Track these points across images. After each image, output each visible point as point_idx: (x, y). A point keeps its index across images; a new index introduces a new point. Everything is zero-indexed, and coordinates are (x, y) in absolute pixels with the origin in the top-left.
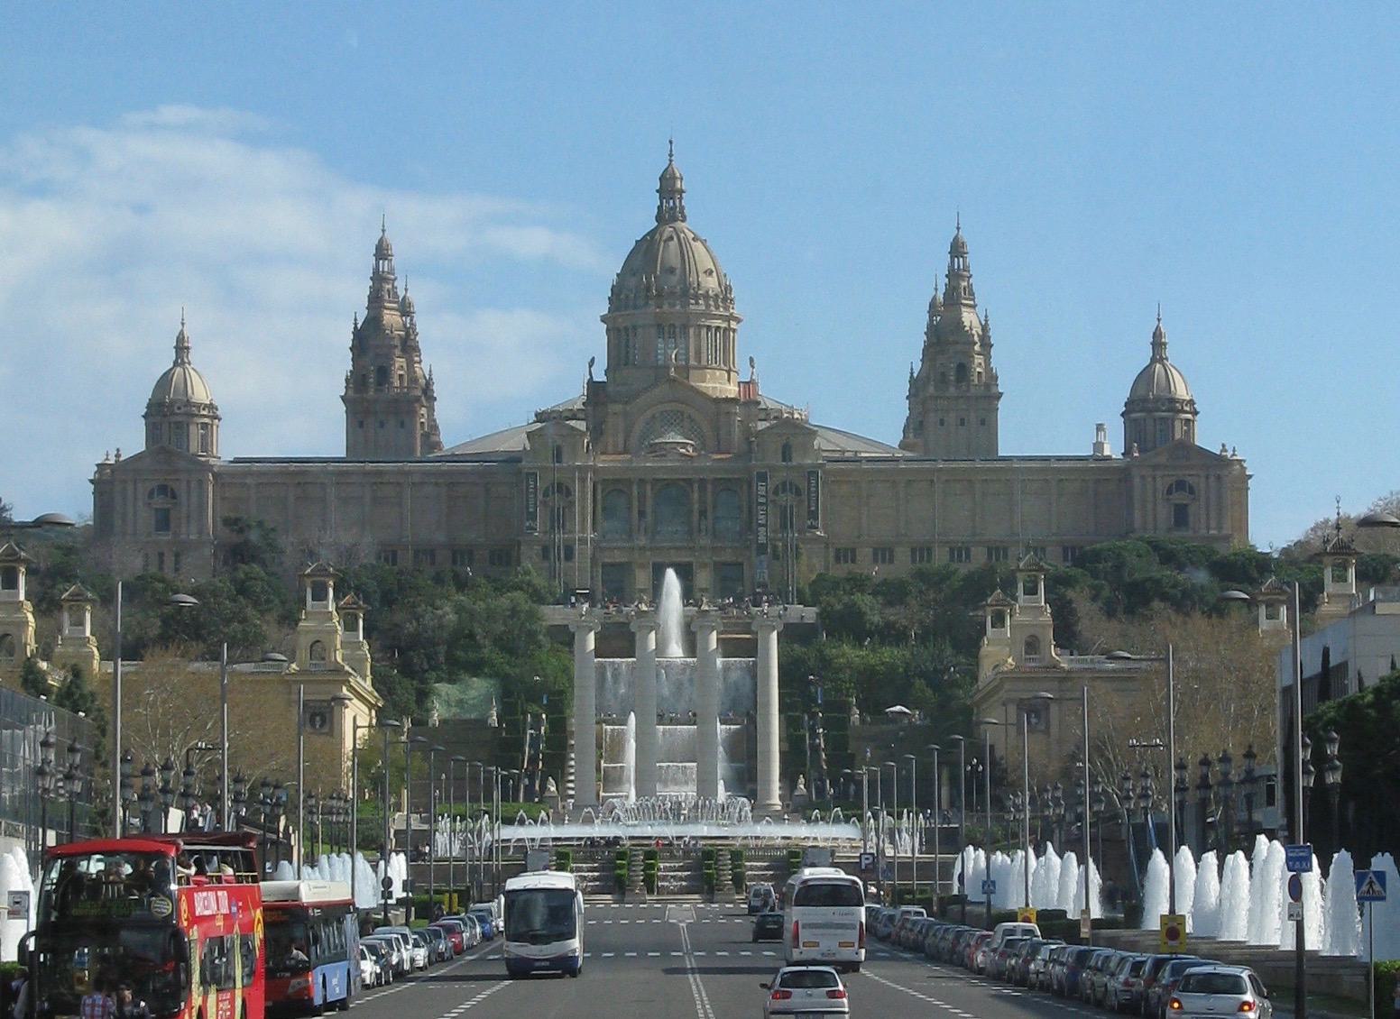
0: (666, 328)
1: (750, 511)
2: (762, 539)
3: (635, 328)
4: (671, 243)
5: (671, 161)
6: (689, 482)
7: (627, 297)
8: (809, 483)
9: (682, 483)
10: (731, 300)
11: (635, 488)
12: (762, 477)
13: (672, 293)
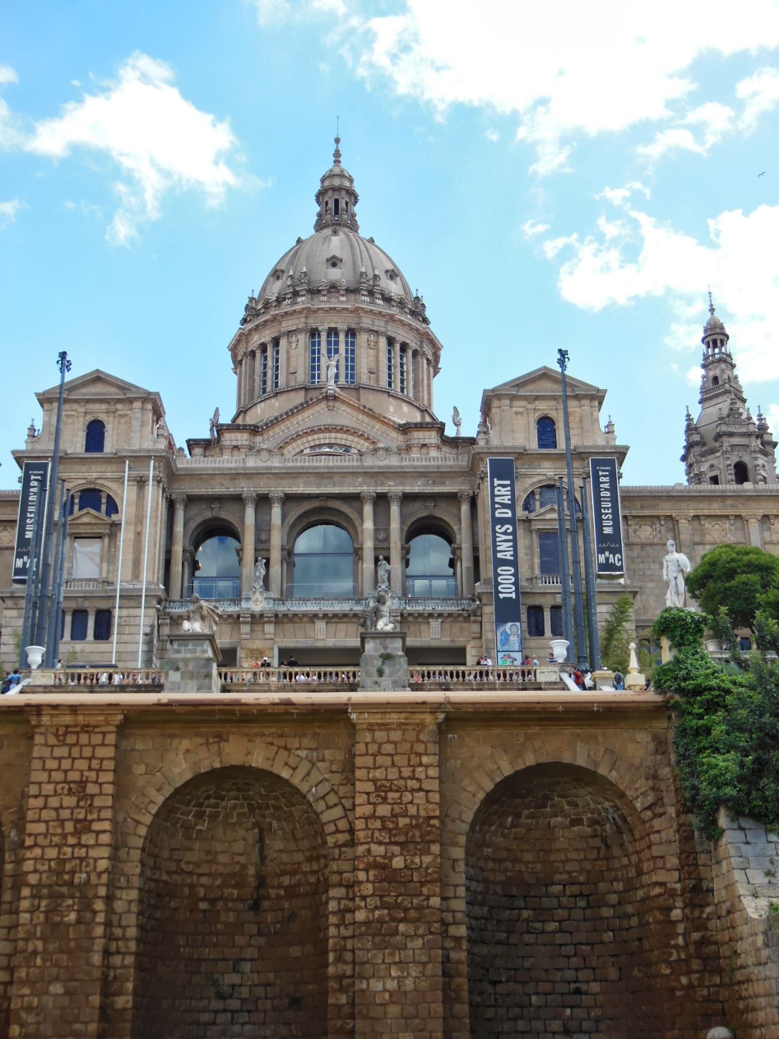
0: (324, 336)
1: (476, 560)
2: (507, 590)
3: (276, 342)
4: (335, 240)
5: (337, 162)
6: (355, 499)
7: (267, 305)
8: (597, 483)
10: (425, 321)
11: (250, 512)
12: (504, 469)
13: (333, 288)
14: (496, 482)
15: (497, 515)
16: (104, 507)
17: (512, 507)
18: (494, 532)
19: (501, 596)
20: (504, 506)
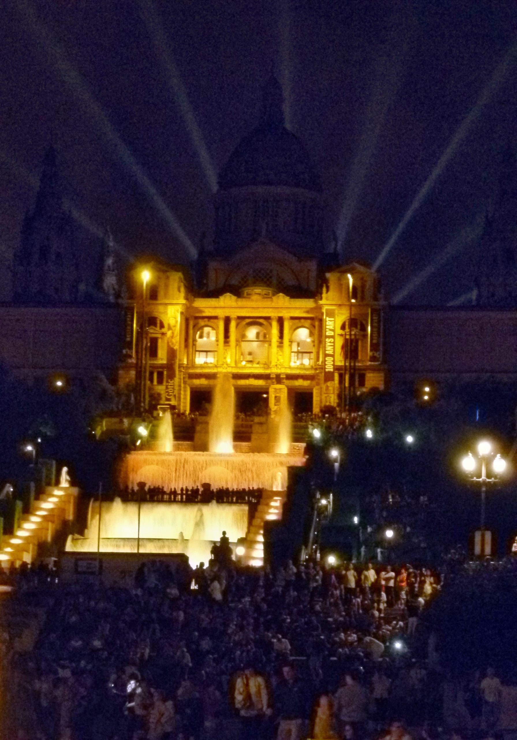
2: (329, 368)
6: (268, 318)
9: (261, 321)
14: (328, 319)
15: (328, 334)
16: (158, 325)
17: (334, 330)
18: (325, 342)
19: (327, 370)
20: (330, 330)
